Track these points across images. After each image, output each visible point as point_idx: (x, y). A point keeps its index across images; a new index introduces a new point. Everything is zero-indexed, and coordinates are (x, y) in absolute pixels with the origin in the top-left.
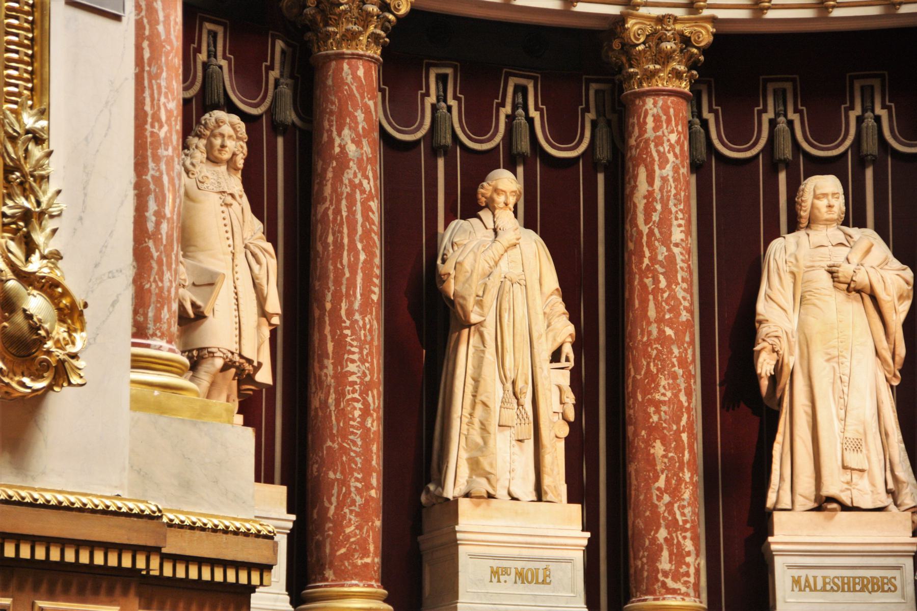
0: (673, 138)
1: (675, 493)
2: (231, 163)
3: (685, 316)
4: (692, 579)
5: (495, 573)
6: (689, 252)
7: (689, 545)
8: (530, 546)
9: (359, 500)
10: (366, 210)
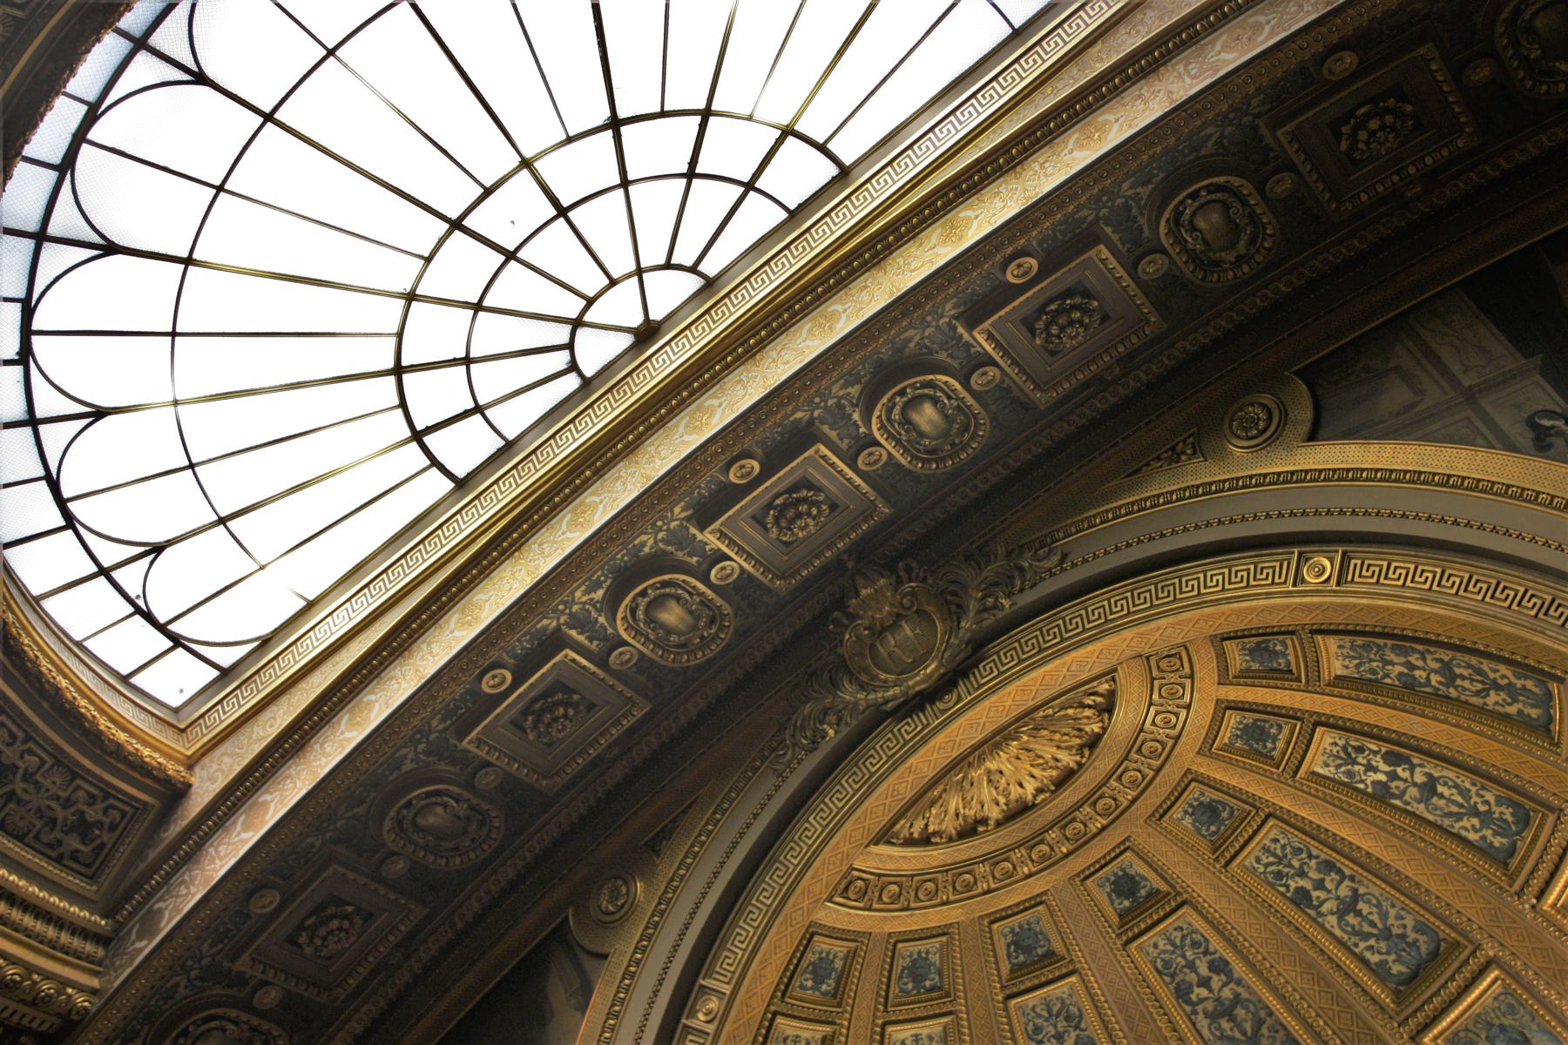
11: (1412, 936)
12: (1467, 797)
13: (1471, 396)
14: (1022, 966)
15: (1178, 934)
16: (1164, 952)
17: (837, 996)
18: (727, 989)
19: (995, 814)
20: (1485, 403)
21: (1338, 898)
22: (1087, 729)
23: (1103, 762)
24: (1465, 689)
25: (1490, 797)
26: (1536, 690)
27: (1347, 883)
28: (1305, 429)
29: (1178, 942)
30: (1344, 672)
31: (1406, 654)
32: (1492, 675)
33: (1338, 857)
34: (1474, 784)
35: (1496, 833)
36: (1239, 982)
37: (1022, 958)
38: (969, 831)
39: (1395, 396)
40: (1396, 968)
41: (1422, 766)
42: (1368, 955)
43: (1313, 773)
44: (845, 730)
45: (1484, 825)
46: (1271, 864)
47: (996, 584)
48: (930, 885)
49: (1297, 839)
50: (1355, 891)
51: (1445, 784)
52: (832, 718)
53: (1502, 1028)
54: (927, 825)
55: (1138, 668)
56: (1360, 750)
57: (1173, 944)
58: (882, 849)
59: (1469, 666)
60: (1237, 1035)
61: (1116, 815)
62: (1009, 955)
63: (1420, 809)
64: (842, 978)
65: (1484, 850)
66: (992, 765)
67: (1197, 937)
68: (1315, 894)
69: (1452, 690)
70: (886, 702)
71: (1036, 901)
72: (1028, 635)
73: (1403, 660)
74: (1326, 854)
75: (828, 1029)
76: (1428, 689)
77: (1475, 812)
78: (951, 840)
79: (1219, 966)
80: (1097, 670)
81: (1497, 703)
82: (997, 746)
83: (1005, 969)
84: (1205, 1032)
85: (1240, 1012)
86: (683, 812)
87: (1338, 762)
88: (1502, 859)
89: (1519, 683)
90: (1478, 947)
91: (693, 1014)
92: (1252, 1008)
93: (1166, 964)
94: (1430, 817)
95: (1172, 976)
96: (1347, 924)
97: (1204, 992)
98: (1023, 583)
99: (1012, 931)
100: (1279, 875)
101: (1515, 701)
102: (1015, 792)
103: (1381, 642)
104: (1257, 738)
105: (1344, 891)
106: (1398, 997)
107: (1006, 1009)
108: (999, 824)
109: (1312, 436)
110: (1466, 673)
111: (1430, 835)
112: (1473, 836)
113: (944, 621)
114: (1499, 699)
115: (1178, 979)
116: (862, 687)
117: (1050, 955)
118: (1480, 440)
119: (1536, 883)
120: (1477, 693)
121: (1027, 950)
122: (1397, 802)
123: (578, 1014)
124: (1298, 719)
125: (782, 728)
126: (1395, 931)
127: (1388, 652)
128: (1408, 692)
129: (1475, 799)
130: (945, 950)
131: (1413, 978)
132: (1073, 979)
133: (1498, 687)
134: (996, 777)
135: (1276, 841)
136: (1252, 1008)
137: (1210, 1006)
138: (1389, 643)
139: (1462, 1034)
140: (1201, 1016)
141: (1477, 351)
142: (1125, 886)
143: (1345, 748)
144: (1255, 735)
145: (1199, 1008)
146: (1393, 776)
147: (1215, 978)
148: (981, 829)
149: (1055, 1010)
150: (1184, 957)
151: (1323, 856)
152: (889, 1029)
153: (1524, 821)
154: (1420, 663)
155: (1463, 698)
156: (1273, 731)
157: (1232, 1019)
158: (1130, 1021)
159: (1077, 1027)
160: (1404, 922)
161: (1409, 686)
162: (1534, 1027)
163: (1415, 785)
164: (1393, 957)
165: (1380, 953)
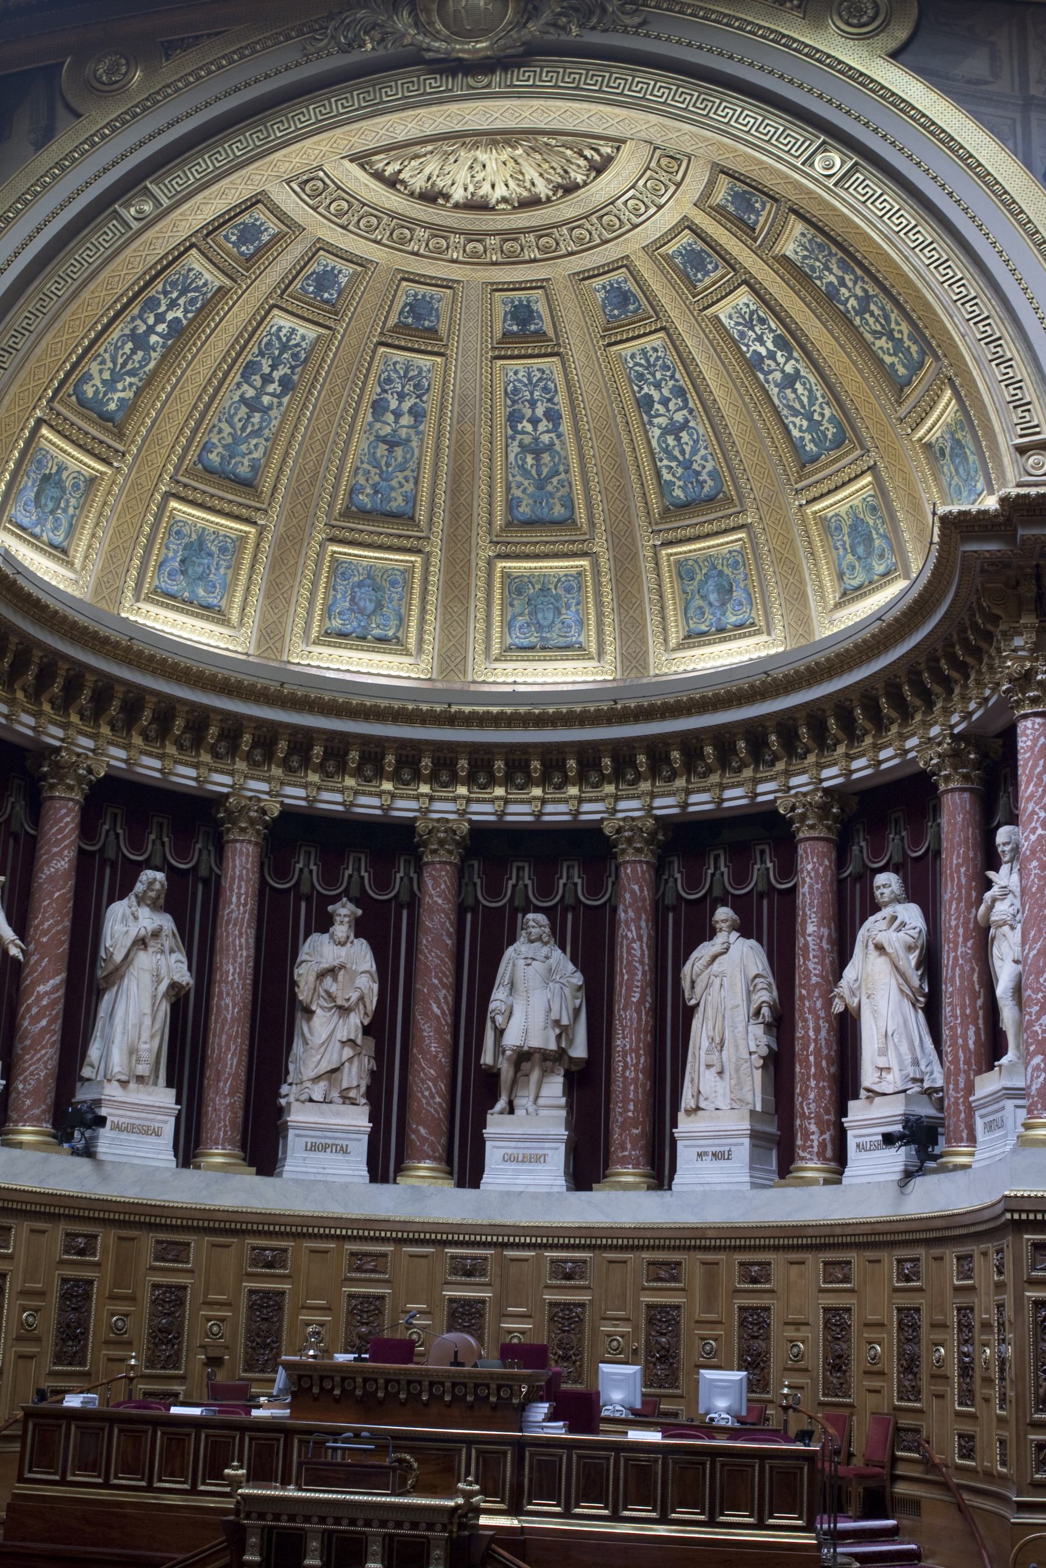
0: (810, 867)
1: (804, 1095)
2: (540, 939)
3: (814, 980)
4: (816, 1150)
5: (700, 1155)
6: (821, 938)
7: (813, 1128)
8: (719, 1137)
9: (620, 1119)
10: (630, 948)
11: (704, 476)
12: (812, 403)
13: (1028, 104)
14: (407, 326)
15: (539, 375)
16: (520, 381)
17: (249, 261)
18: (166, 202)
19: (458, 195)
20: (1034, 116)
21: (671, 419)
22: (573, 174)
23: (568, 209)
24: (867, 324)
25: (827, 412)
26: (915, 355)
27: (685, 412)
28: (893, 45)
29: (535, 380)
30: (792, 256)
31: (845, 272)
32: (893, 326)
33: (691, 388)
34: (823, 397)
35: (812, 440)
36: (559, 436)
37: (410, 320)
38: (431, 197)
39: (976, 65)
40: (678, 493)
41: (797, 361)
42: (664, 471)
43: (717, 317)
44: (381, 51)
45: (809, 430)
46: (641, 365)
47: (576, 10)
48: (374, 221)
49: (672, 358)
50: (687, 421)
51: (804, 384)
52: (377, 34)
53: (721, 573)
54: (400, 171)
55: (645, 150)
56: (762, 321)
57: (530, 379)
58: (354, 169)
59: (883, 309)
60: (534, 472)
61: (550, 255)
62: (401, 313)
63: (774, 391)
64: (261, 250)
65: (796, 447)
66: (482, 156)
67: (551, 385)
68: (657, 406)
69: (858, 319)
70: (429, 50)
71: (447, 284)
72: (578, 72)
73: (840, 274)
74: (684, 382)
75: (228, 282)
76: (841, 307)
77: (809, 417)
78: (412, 194)
79: (552, 416)
80: (610, 132)
81: (881, 348)
82: (495, 143)
83: (392, 320)
84: (512, 457)
85: (546, 457)
86: (209, 36)
87: (741, 320)
88: (805, 462)
89: (907, 343)
90: (743, 511)
91: (127, 205)
92: (557, 460)
93: (516, 391)
94: (777, 402)
95: (514, 402)
96: (665, 441)
97: (529, 428)
98: (599, 22)
99: (416, 294)
100: (641, 376)
101: (895, 354)
102: (486, 189)
103: (834, 249)
104: (696, 262)
105: (679, 417)
106: (666, 513)
107: (374, 352)
108: (457, 206)
109: (895, 55)
110: (877, 312)
111: (767, 414)
112: (796, 433)
113: (515, 13)
114: (885, 346)
115: (516, 407)
116: (417, 24)
117: (432, 332)
118: (1010, 143)
119: (815, 492)
120: (874, 332)
121: (418, 317)
122: (761, 377)
123: (31, 148)
124: (734, 269)
125: (331, 17)
126: (695, 466)
127: (834, 261)
129: (817, 407)
130: (354, 277)
131: (684, 507)
132: (439, 360)
133: (891, 337)
134: (478, 167)
135: (655, 350)
136: (557, 460)
137: (527, 440)
138: (840, 254)
139: (690, 563)
140: (516, 443)
142: (522, 314)
143: (752, 313)
144: (695, 260)
145: (519, 437)
146: (772, 356)
147: (545, 422)
148: (441, 201)
149: (411, 374)
150: (532, 394)
151: (681, 383)
152: (276, 312)
153: (839, 442)
154: (850, 284)
155: (862, 329)
156: (710, 267)
157: (537, 459)
158: (461, 417)
159: (419, 397)
160: (706, 463)
161: (830, 296)
162: (742, 585)
163: (783, 371)
164: (681, 483)
165: (674, 475)
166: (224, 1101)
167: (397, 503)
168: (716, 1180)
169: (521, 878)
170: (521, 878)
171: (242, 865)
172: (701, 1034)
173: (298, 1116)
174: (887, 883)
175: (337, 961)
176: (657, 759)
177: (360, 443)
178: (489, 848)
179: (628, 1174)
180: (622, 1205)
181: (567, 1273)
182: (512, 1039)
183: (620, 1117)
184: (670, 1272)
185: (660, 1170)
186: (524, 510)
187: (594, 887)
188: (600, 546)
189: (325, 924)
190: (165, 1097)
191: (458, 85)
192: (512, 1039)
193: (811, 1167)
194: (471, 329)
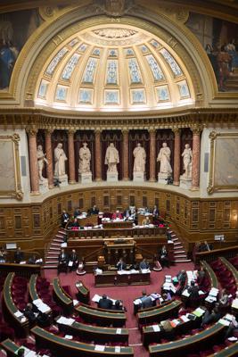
39: (196, 27)
72: (132, 21)
128: (166, 61)
141: (209, 29)
142: (113, 53)
166: (73, 174)
167: (90, 81)
168: (139, 178)
169: (108, 137)
170: (108, 137)
171: (71, 140)
172: (136, 161)
173: (82, 175)
174: (165, 144)
175: (85, 152)
176: (130, 122)
177: (85, 72)
178: (105, 133)
179: (126, 179)
180: (126, 183)
181: (119, 192)
182: (110, 161)
183: (125, 170)
184: (133, 192)
185: (131, 178)
186: (110, 82)
187: (119, 137)
188: (121, 88)
189: (83, 146)
190: (66, 176)
191: (113, 20)
192: (110, 161)
193: (152, 179)
194: (105, 55)
